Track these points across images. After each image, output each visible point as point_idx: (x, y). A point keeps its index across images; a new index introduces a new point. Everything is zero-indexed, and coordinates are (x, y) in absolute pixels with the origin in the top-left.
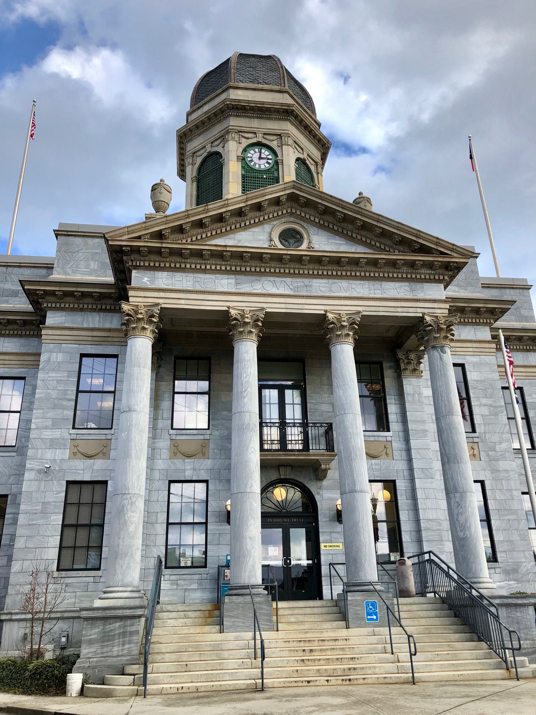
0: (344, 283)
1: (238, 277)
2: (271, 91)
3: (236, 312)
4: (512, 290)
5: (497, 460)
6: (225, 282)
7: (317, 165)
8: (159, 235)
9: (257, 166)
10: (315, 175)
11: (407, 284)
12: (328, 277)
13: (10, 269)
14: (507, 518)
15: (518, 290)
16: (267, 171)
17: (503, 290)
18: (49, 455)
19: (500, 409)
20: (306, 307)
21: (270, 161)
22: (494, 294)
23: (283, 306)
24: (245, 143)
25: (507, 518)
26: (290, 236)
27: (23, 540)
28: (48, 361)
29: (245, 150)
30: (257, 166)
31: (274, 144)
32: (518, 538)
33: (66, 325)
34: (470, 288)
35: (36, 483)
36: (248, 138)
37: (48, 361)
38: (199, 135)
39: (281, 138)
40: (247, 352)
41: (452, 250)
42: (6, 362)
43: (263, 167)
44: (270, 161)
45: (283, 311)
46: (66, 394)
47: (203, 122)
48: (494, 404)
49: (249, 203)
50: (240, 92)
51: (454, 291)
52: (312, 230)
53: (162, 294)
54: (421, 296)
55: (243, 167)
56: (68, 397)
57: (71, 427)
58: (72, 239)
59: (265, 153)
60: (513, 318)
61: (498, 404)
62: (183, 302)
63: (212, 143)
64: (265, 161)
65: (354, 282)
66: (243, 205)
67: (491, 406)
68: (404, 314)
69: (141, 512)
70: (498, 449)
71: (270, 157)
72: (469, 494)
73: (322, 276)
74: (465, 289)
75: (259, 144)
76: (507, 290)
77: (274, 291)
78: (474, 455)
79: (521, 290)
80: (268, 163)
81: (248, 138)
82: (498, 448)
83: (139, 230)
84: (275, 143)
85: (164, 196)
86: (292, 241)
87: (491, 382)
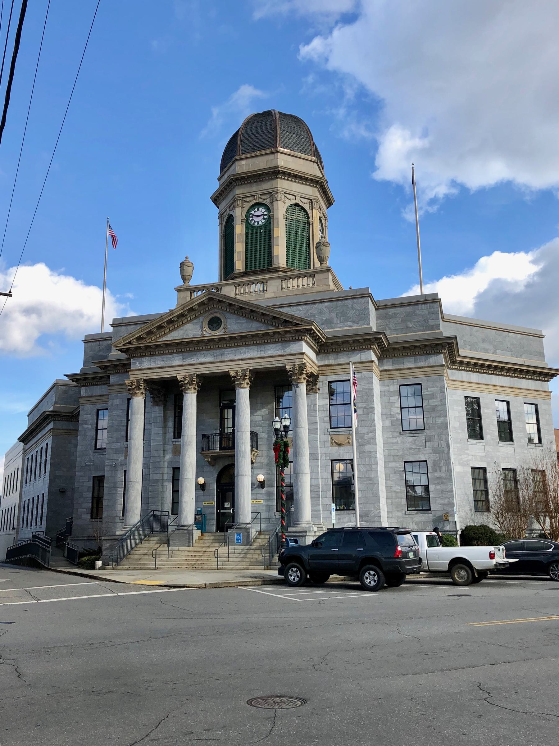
0: (243, 349)
1: (184, 354)
2: (266, 154)
3: (181, 377)
4: (423, 306)
5: (364, 445)
6: (177, 360)
7: (312, 202)
8: (139, 338)
9: (256, 223)
10: (309, 212)
11: (280, 344)
12: (232, 347)
13: (101, 342)
14: (366, 482)
15: (428, 305)
16: (263, 225)
17: (416, 307)
18: (115, 457)
19: (370, 410)
20: (220, 368)
21: (266, 217)
22: (408, 310)
23: (208, 369)
24: (247, 206)
25: (366, 482)
26: (214, 323)
27: (107, 501)
28: (112, 405)
29: (248, 212)
30: (256, 223)
31: (267, 202)
32: (371, 495)
33: (120, 382)
34: (361, 322)
35: (110, 472)
36: (249, 202)
37: (112, 405)
38: (223, 199)
39: (272, 195)
40: (187, 400)
41: (301, 321)
42: (104, 400)
43: (260, 223)
44: (266, 217)
45: (208, 372)
46: (121, 423)
47: (223, 191)
48: (367, 407)
49: (185, 309)
50: (243, 162)
51: (350, 326)
52: (228, 315)
53: (145, 371)
54: (288, 351)
55: (246, 227)
56: (123, 424)
57: (125, 441)
58: (119, 328)
59: (262, 210)
60: (422, 328)
61: (370, 406)
62: (155, 374)
63: (229, 207)
64: (262, 217)
65: (249, 347)
66: (182, 311)
67: (365, 408)
68: (277, 365)
69: (138, 490)
70: (366, 438)
71: (265, 213)
72: (301, 475)
73: (229, 347)
74: (358, 324)
75: (257, 205)
76: (420, 306)
77: (203, 360)
78: (349, 443)
79: (431, 305)
80: (264, 219)
81: (249, 202)
82: (366, 437)
83: (128, 338)
84: (268, 200)
85: (188, 271)
86: (215, 325)
87: (367, 391)
